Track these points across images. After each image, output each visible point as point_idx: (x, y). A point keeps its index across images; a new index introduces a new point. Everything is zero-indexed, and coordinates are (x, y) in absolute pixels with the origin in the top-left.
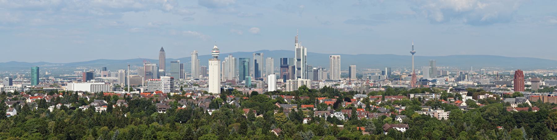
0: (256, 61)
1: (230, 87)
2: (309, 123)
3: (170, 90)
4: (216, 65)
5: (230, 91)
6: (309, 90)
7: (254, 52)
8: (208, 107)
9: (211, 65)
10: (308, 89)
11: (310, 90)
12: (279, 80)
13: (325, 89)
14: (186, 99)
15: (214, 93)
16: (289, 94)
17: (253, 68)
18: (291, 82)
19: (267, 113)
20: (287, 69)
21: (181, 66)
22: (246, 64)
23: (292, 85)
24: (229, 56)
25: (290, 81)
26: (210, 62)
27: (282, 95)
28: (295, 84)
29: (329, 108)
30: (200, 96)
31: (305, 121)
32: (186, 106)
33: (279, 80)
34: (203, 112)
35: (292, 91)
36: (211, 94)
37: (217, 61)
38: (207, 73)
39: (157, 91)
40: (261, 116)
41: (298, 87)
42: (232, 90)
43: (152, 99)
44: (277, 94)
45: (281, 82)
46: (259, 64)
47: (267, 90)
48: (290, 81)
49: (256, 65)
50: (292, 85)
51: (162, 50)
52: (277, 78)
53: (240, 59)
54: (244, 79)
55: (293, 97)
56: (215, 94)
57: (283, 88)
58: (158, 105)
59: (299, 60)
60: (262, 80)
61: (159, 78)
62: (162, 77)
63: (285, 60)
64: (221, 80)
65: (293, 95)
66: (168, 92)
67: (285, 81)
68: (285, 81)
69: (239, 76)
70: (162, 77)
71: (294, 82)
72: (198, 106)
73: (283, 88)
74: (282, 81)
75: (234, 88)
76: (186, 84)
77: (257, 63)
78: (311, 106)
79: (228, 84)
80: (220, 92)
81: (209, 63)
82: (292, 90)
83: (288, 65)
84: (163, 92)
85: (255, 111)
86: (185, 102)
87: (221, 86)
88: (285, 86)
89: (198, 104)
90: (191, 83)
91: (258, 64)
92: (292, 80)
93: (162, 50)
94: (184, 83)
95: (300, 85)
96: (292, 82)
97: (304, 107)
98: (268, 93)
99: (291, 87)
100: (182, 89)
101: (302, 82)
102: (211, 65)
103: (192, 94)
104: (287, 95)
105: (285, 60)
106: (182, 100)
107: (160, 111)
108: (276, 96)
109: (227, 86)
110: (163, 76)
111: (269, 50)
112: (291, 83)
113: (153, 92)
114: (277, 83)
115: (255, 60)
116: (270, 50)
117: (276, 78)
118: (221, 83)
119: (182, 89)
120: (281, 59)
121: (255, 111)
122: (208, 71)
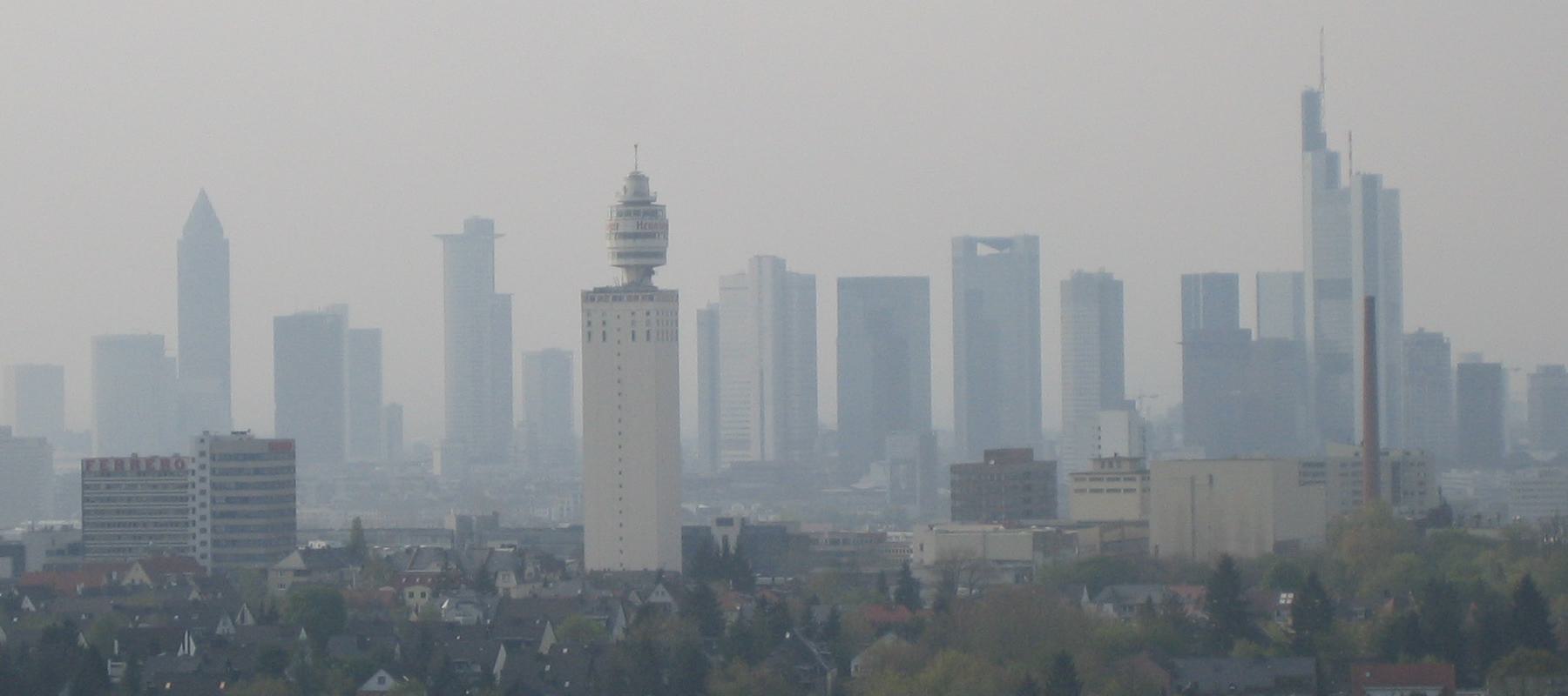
53: (843, 284)
84: (207, 563)
89: (488, 669)
113: (127, 567)
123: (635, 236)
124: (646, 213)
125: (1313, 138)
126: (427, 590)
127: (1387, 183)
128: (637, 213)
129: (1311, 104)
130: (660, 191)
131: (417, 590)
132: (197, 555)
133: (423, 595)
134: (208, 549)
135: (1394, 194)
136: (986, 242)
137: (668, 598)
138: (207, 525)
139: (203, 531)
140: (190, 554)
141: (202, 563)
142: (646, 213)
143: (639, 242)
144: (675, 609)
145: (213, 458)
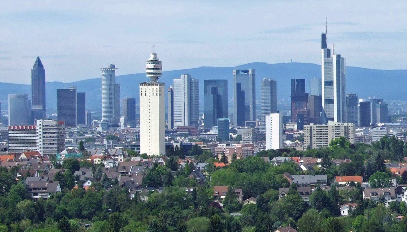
0: (239, 85)
1: (186, 141)
2: (354, 214)
3: (56, 150)
4: (155, 94)
5: (185, 150)
6: (352, 146)
7: (232, 68)
8: (141, 183)
9: (144, 93)
10: (348, 143)
11: (353, 145)
12: (288, 126)
13: (384, 143)
14: (91, 168)
15: (150, 153)
16: (310, 154)
17: (232, 100)
18: (313, 128)
19: (264, 195)
20: (305, 103)
21: (82, 96)
22: (220, 92)
23: (316, 135)
24: (182, 75)
25: (311, 127)
26: (143, 89)
27: (295, 156)
28: (323, 134)
29: (394, 181)
30: (121, 160)
31: (345, 211)
32: (91, 183)
33: (288, 126)
34: (129, 193)
35: (316, 148)
36: (145, 156)
37: (158, 87)
38: (136, 113)
39: (28, 150)
40: (253, 202)
41: (329, 142)
42: (190, 146)
43: (16, 169)
44: (286, 156)
45: (293, 130)
46: (246, 94)
47: (265, 147)
48: (311, 127)
49: (241, 95)
50: (316, 135)
51: (39, 64)
52: (285, 120)
53: (207, 82)
54: (215, 124)
55: (319, 160)
56: (153, 156)
57: (297, 141)
58: (32, 182)
59: (329, 83)
60: (253, 125)
61: (32, 122)
62: (38, 121)
63: (301, 83)
64: (167, 127)
65: (319, 157)
66: (53, 154)
67: (300, 127)
68: (300, 127)
69: (203, 117)
70: (39, 122)
71: (319, 130)
72: (117, 182)
73: (297, 141)
74: (295, 127)
75: (194, 143)
76: (91, 136)
77: (242, 89)
78: (357, 179)
79: (181, 135)
80: (164, 153)
81: (140, 90)
82: (316, 145)
83: (307, 94)
84: (42, 153)
85: (240, 190)
86: (89, 173)
87: (167, 138)
88: (301, 139)
89: (116, 179)
90: (100, 134)
91: (244, 92)
92: (315, 125)
93: (39, 64)
94: (87, 133)
95: (331, 137)
96: (316, 128)
97: (342, 181)
98: (265, 153)
99: (315, 140)
100: (82, 148)
101: (337, 128)
102: (144, 93)
103: (104, 158)
104: (306, 157)
105: (301, 83)
106: (82, 169)
107: (36, 194)
108: (282, 159)
109: (179, 138)
110: (41, 120)
111: (265, 64)
112: (314, 132)
113: (20, 154)
114: (284, 131)
115: (237, 84)
116: (270, 62)
117: (281, 121)
118: (167, 133)
119: (82, 148)
120: (293, 81)
121: (240, 190)
122: (139, 109)
123: (153, 69)
124: (156, 63)
125: (324, 45)
126: (100, 160)
127: (342, 56)
128: (154, 63)
129: (324, 36)
130: (160, 58)
131: (97, 159)
132: (39, 151)
133: (99, 161)
134: (42, 149)
135: (343, 59)
136: (243, 71)
137: (163, 161)
138: (42, 143)
139: (40, 145)
140: (37, 151)
141: (40, 153)
142: (156, 63)
143: (155, 71)
144: (164, 164)
145: (43, 126)
